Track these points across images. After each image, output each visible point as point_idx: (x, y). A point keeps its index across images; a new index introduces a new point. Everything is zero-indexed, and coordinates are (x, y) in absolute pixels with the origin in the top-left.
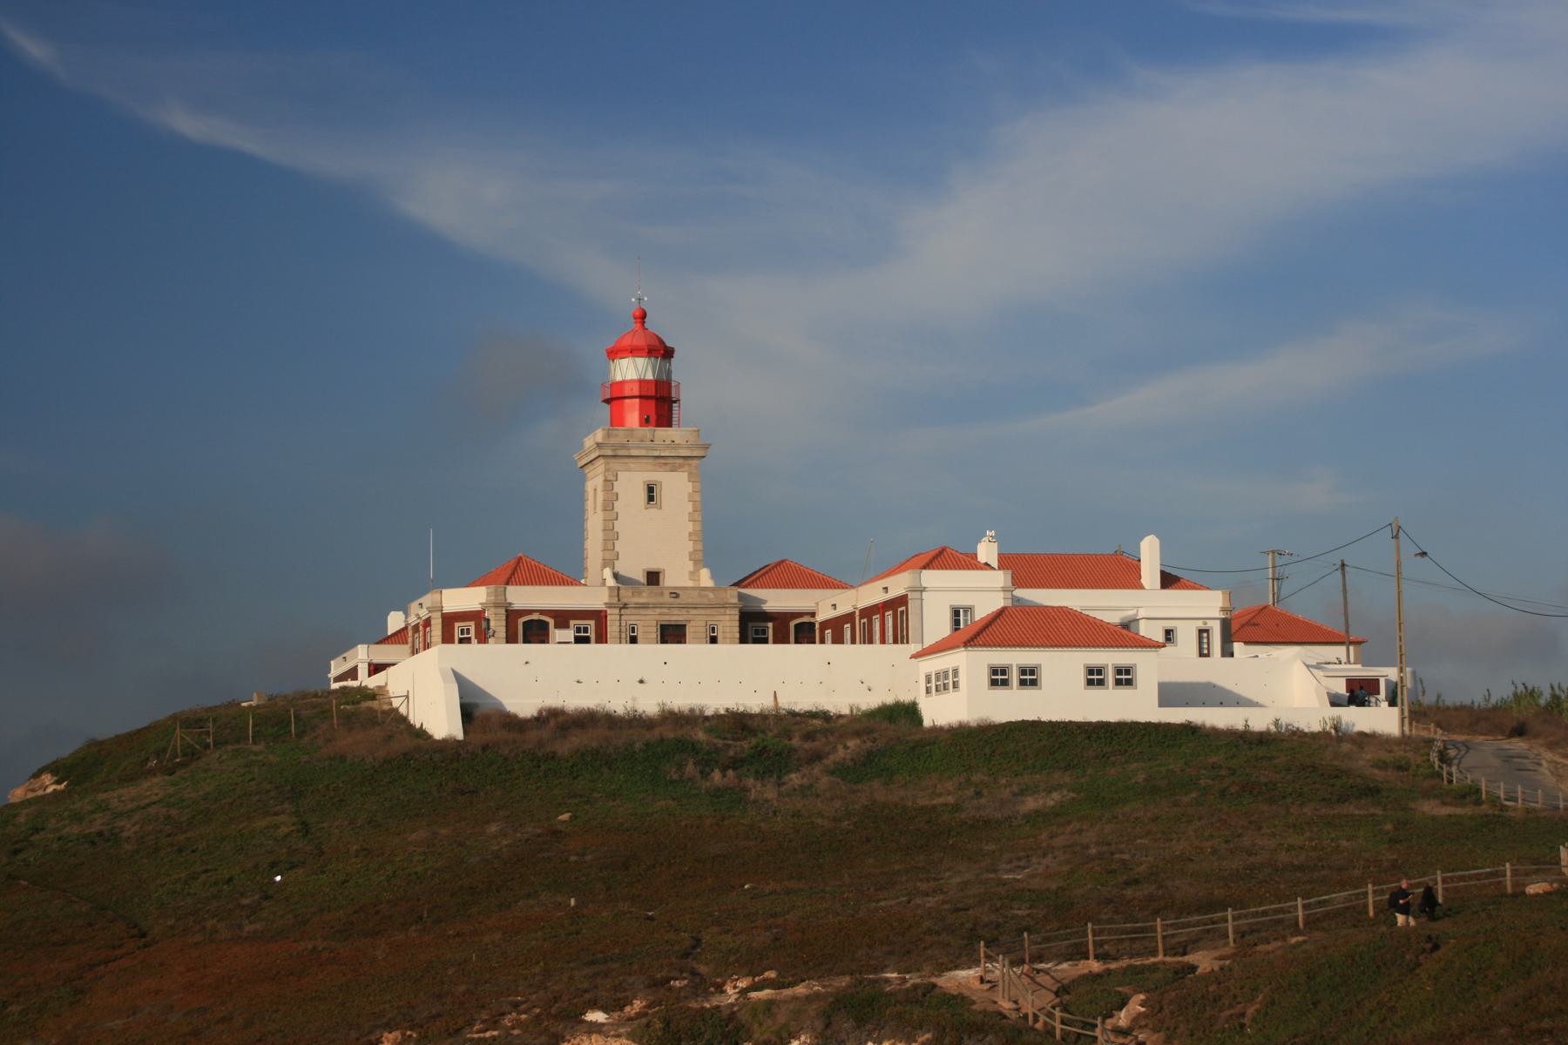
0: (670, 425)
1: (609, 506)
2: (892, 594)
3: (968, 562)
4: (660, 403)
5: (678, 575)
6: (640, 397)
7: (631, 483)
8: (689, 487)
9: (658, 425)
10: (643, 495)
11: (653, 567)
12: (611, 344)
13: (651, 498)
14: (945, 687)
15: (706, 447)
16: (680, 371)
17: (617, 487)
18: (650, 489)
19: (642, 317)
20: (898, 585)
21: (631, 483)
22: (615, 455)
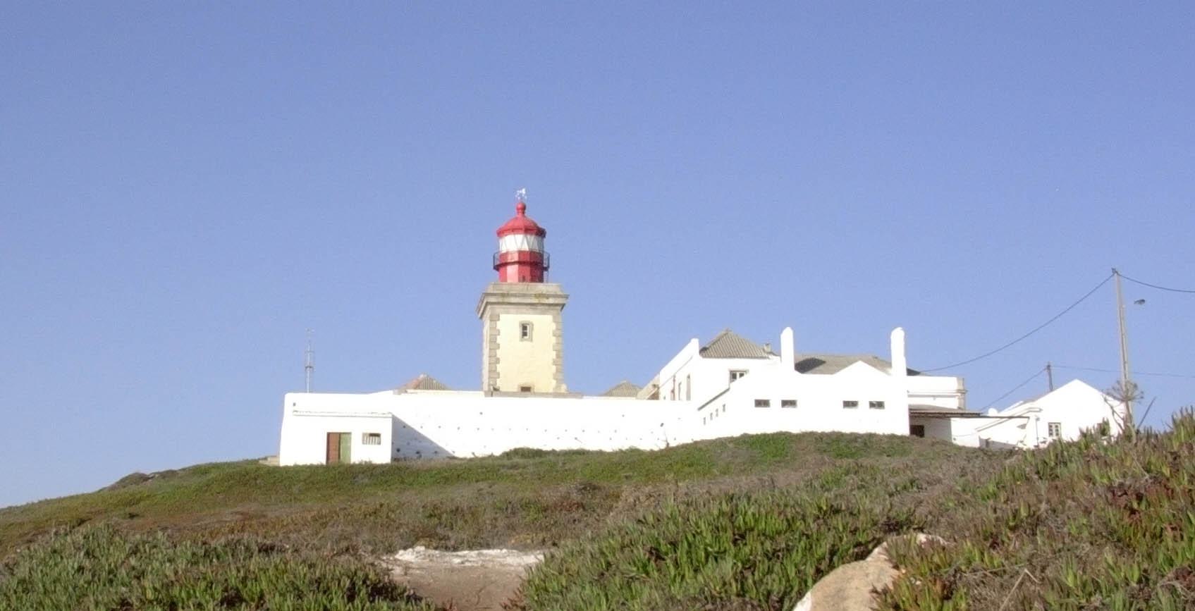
0: (541, 280)
4: (534, 266)
6: (519, 263)
7: (509, 322)
8: (554, 326)
9: (533, 280)
10: (519, 331)
11: (525, 382)
12: (502, 224)
13: (525, 334)
15: (566, 297)
16: (550, 246)
17: (499, 325)
18: (524, 327)
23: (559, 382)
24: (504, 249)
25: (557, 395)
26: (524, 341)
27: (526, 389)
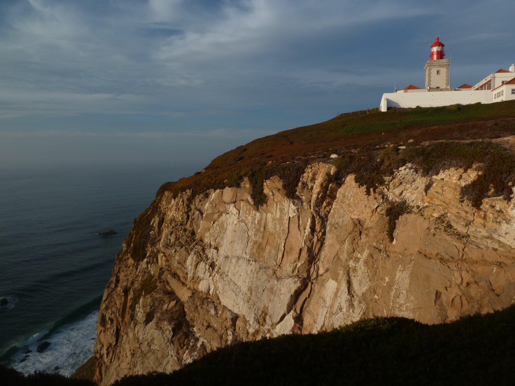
1: (429, 75)
2: (487, 80)
3: (508, 72)
5: (443, 86)
7: (434, 71)
8: (446, 71)
10: (436, 72)
11: (438, 86)
12: (432, 44)
14: (500, 96)
19: (438, 39)
20: (488, 78)
21: (434, 71)
22: (431, 66)
23: (447, 85)
24: (432, 51)
25: (447, 90)
26: (438, 74)
27: (438, 88)
